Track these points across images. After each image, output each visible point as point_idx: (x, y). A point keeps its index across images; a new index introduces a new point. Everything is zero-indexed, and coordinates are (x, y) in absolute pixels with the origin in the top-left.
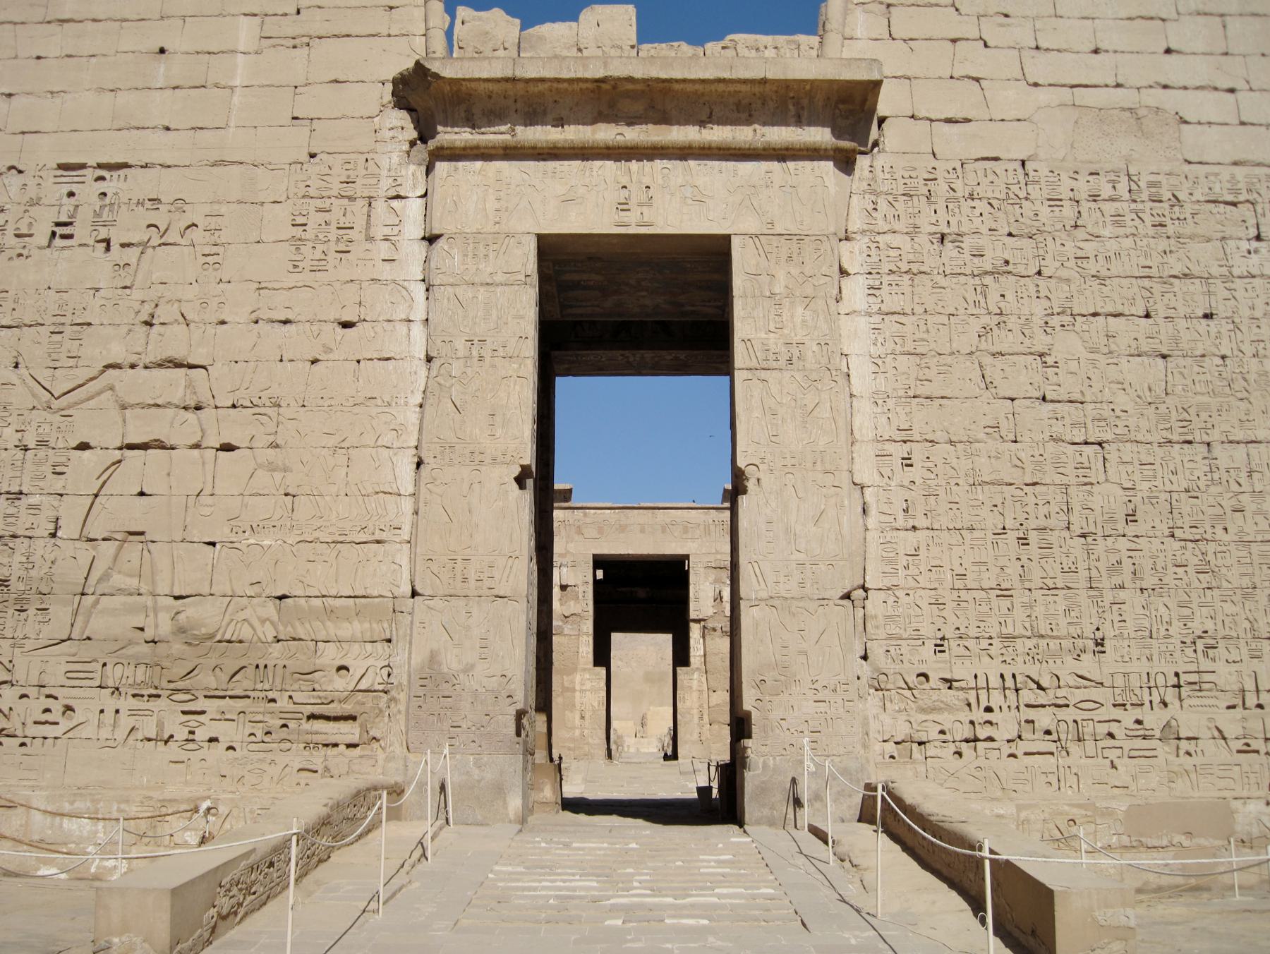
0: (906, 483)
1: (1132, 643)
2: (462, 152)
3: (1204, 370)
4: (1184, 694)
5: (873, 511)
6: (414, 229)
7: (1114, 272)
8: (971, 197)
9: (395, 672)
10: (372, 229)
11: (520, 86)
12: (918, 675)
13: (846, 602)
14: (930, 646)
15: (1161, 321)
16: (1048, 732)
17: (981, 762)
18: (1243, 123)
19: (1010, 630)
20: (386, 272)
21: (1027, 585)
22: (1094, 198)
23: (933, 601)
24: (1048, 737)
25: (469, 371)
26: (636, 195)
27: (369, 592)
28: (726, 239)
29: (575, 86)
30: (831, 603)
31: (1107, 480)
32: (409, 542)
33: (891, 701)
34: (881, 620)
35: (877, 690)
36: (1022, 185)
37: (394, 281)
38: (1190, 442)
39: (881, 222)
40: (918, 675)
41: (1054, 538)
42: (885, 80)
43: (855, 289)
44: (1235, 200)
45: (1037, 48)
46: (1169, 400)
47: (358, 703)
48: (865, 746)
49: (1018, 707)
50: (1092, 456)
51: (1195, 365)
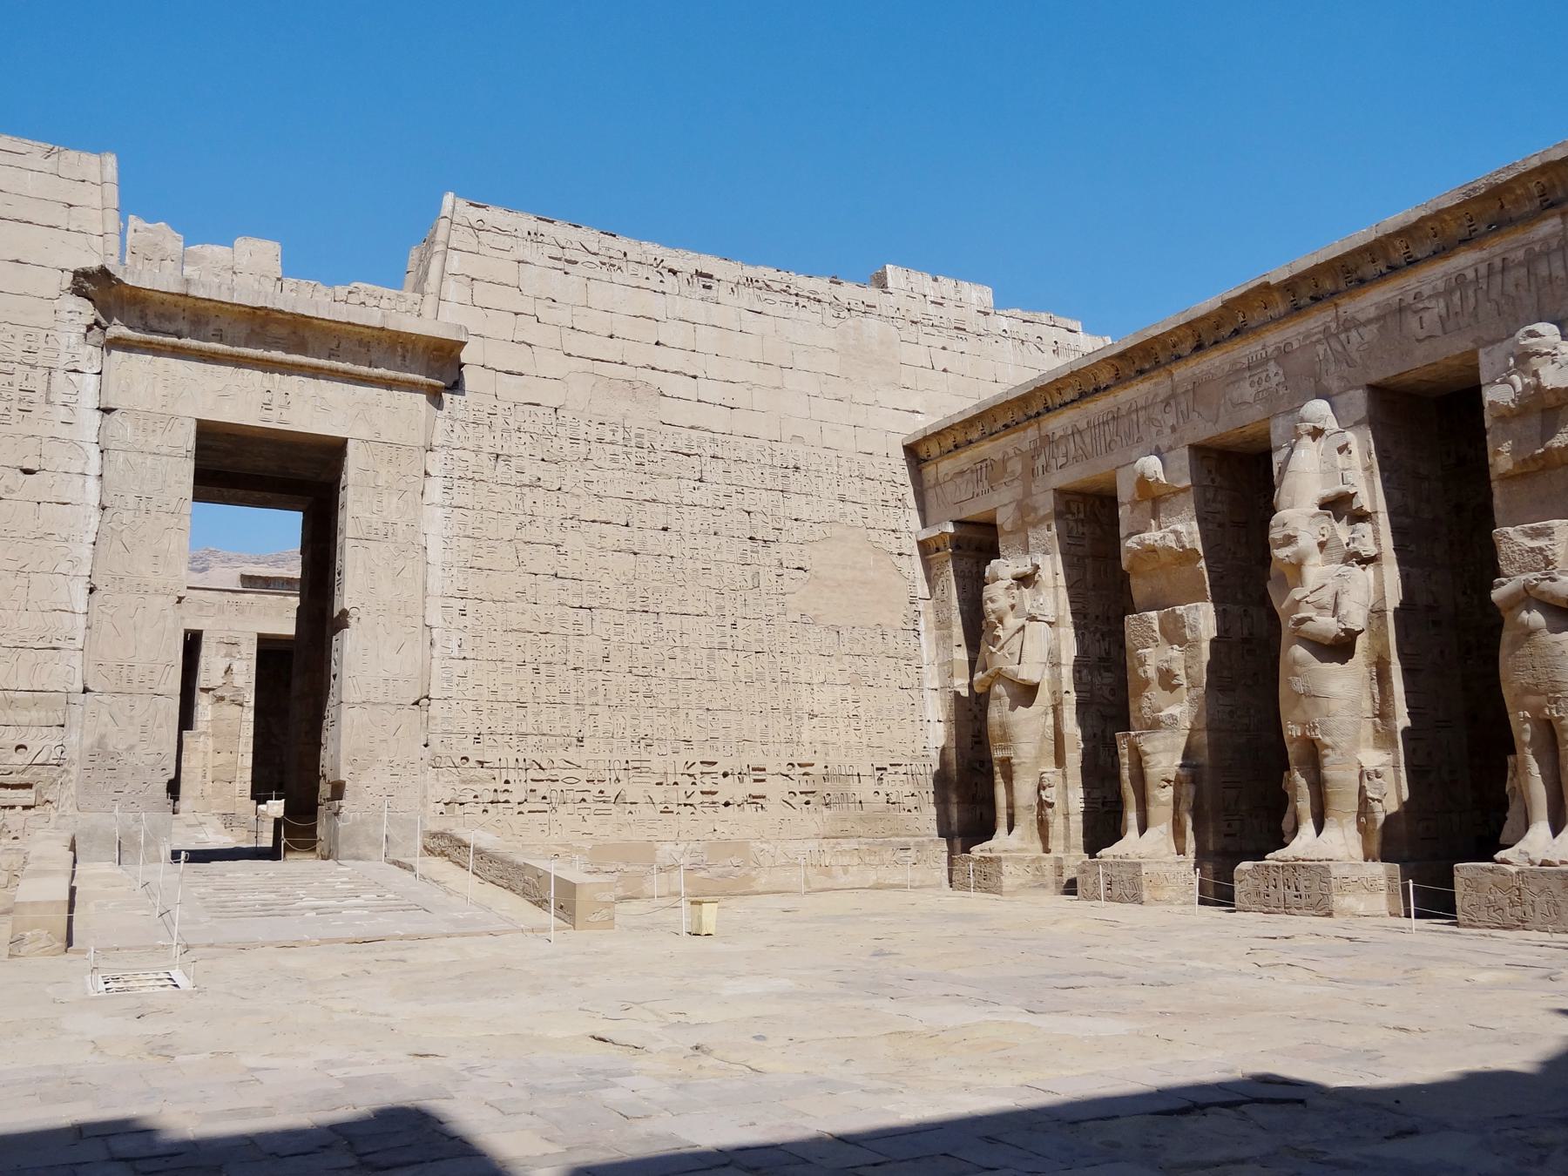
0: (461, 628)
1: (601, 741)
2: (136, 344)
3: (659, 565)
4: (631, 775)
5: (438, 646)
6: (89, 400)
7: (608, 493)
8: (519, 430)
9: (68, 750)
10: (52, 395)
11: (189, 300)
12: (462, 758)
13: (416, 707)
14: (471, 738)
15: (636, 530)
16: (544, 798)
17: (500, 817)
18: (699, 401)
19: (523, 729)
20: (64, 432)
21: (537, 700)
22: (600, 440)
23: (475, 709)
24: (544, 801)
25: (137, 520)
26: (278, 400)
27: (45, 688)
28: (345, 441)
29: (236, 308)
30: (406, 708)
31: (592, 633)
32: (82, 650)
33: (443, 775)
34: (439, 721)
35: (434, 768)
36: (554, 425)
37: (72, 441)
38: (647, 612)
39: (455, 440)
40: (462, 758)
41: (556, 669)
42: (471, 341)
43: (435, 489)
44: (690, 453)
45: (572, 328)
46: (636, 582)
47: (34, 774)
48: (424, 805)
49: (526, 781)
50: (584, 616)
51: (654, 560)
